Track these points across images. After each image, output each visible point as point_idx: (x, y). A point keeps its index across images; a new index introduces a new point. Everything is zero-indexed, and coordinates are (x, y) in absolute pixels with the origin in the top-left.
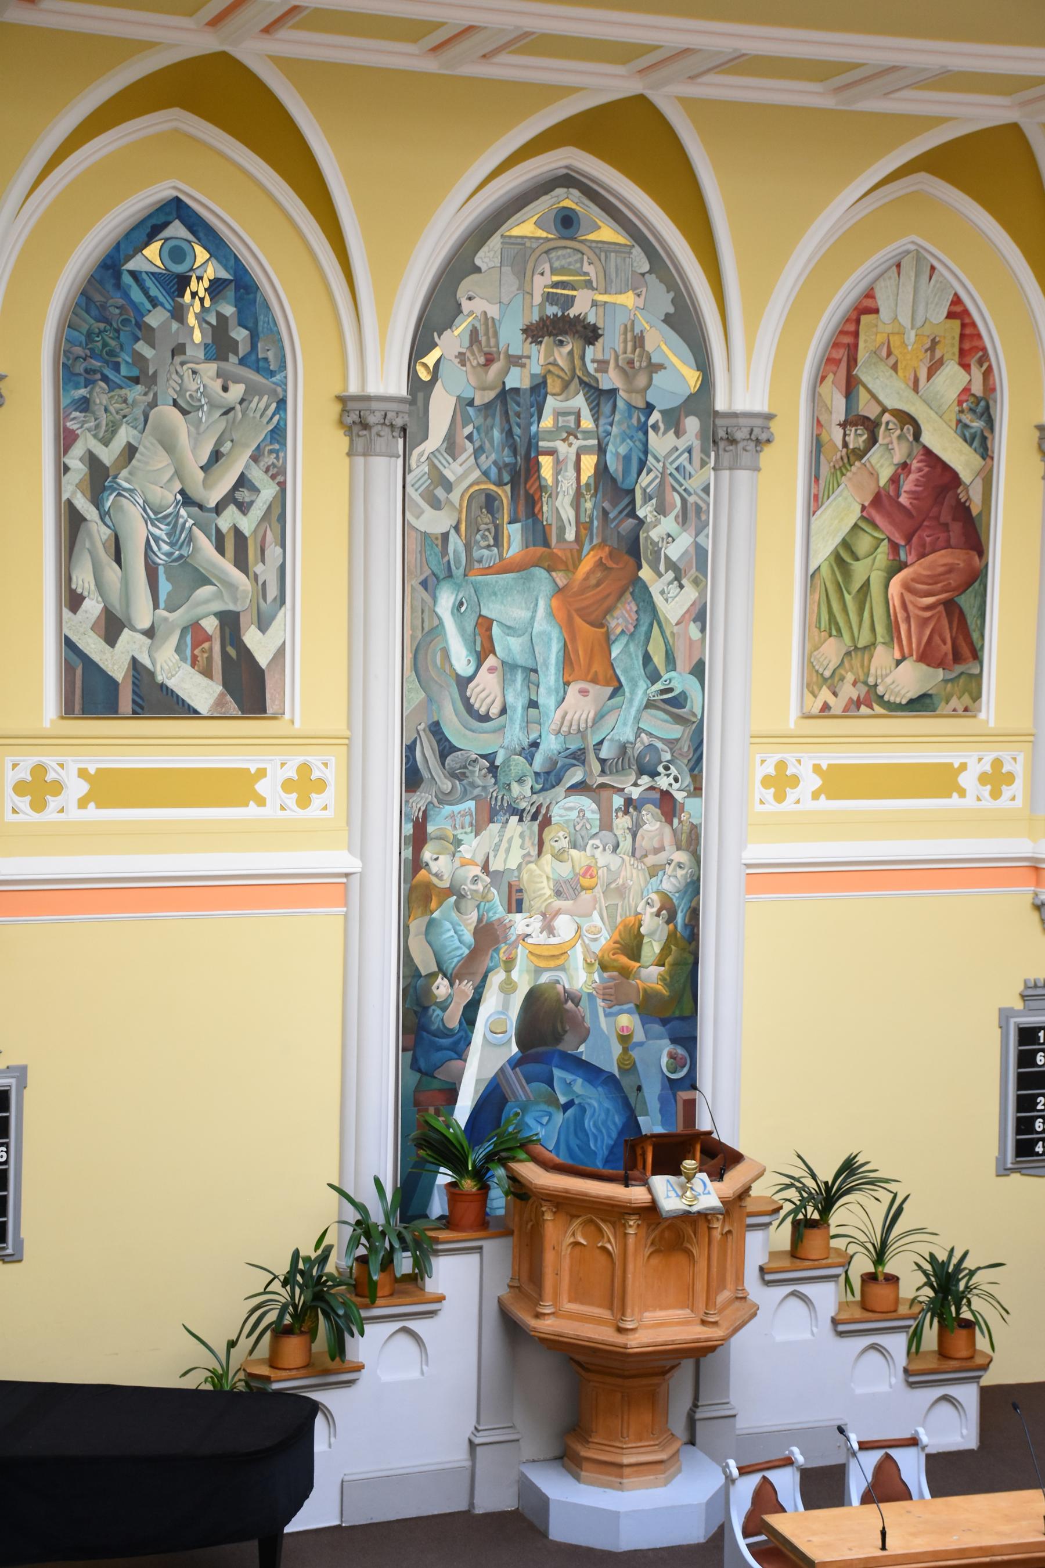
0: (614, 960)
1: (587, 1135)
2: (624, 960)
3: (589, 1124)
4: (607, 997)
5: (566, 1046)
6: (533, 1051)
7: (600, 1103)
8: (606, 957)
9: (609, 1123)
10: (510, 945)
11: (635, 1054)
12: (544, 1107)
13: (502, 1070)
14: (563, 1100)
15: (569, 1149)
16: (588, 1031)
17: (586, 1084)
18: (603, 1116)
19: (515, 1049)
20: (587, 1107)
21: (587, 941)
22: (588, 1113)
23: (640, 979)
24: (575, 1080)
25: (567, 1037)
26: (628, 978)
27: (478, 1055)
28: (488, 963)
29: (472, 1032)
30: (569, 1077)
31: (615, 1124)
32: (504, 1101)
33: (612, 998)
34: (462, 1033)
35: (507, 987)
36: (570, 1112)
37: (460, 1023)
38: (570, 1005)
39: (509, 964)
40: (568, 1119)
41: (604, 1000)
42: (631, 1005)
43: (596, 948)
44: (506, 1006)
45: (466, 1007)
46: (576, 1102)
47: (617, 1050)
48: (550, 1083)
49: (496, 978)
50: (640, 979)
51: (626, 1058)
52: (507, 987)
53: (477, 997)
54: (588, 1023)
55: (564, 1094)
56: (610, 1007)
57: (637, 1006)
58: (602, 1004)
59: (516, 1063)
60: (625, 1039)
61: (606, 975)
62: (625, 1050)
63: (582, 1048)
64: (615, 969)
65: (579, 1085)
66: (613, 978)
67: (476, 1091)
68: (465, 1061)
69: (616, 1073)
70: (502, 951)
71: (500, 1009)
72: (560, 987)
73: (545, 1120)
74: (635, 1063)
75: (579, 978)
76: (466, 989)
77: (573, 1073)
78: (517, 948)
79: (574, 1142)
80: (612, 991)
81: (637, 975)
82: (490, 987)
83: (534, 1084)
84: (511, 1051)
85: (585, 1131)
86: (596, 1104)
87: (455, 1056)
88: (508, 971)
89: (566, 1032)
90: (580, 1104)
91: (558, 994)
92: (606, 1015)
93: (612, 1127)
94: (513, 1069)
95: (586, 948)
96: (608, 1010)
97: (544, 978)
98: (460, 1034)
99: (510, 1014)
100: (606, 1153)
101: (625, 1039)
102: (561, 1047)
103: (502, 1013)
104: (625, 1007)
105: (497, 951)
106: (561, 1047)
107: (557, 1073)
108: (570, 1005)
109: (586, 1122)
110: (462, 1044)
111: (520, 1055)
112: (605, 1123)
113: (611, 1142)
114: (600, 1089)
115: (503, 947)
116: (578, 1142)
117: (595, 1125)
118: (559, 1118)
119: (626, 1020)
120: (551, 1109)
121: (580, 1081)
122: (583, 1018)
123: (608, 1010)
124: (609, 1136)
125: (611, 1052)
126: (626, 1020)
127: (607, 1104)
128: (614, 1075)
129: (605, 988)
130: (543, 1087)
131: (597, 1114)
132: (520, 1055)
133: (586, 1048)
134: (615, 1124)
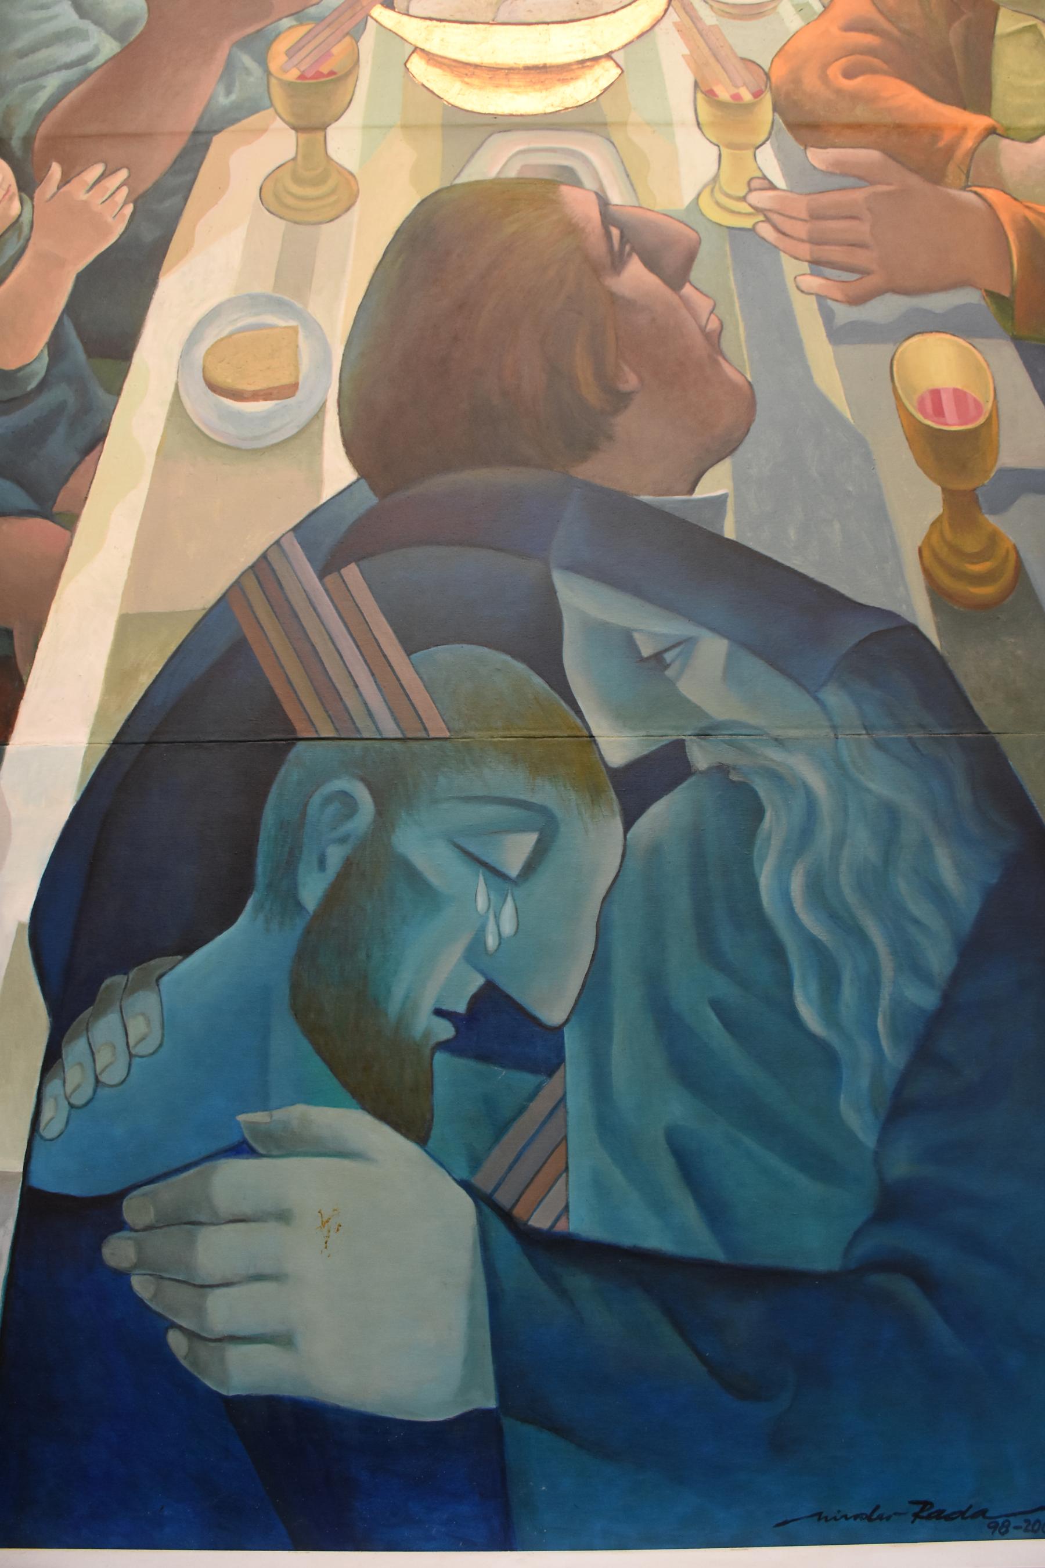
0: (855, 97)
1: (777, 951)
2: (907, 99)
3: (780, 884)
4: (835, 253)
5: (633, 462)
6: (440, 484)
7: (842, 776)
8: (811, 82)
9: (903, 886)
10: (320, 20)
11: (1015, 526)
12: (504, 778)
13: (263, 569)
14: (618, 746)
15: (664, 1017)
16: (748, 401)
17: (755, 667)
18: (862, 844)
19: (337, 472)
20: (762, 788)
21: (708, 17)
22: (776, 826)
23: (1000, 186)
24: (686, 644)
25: (627, 423)
26: (935, 176)
27: (138, 497)
28: (207, 90)
29: (116, 391)
30: (652, 627)
31: (936, 892)
32: (271, 740)
33: (861, 258)
34: (60, 393)
35: (309, 194)
36: (663, 814)
37: (56, 346)
38: (635, 277)
39: (315, 104)
40: (655, 851)
41: (817, 264)
42: (970, 297)
43: (758, 42)
44: (294, 277)
45: (79, 277)
46: (700, 757)
47: (916, 504)
48: (539, 644)
49: (251, 157)
50: (1000, 186)
51: (971, 544)
52: (309, 194)
53: (149, 234)
54: (741, 357)
55: (623, 715)
56: (857, 300)
57: (992, 295)
58: (813, 282)
59: (334, 541)
60: (953, 450)
61: (819, 157)
62: (962, 507)
63: (716, 483)
64: (858, 131)
65: (710, 673)
66: (864, 177)
67: (117, 675)
68: (69, 522)
69: (924, 617)
70: (279, 50)
71: (264, 286)
72: (580, 204)
73: (515, 851)
74: (1020, 567)
75: (684, 169)
76: (96, 199)
77: (670, 607)
78: (356, 33)
79: (693, 987)
80: (862, 230)
81: (979, 169)
82: (221, 188)
83: (443, 654)
84: (318, 482)
85: (764, 924)
86: (816, 781)
87: (24, 501)
88: (311, 126)
89: (620, 400)
90: (722, 769)
91: (572, 229)
92: (837, 334)
93: (920, 909)
94: (328, 567)
95: (708, 54)
96: (844, 314)
97: (494, 162)
98: (60, 393)
99: (316, 308)
100: (895, 1057)
101: (953, 450)
102: (601, 470)
103: (278, 305)
104: (939, 302)
105: (259, 45)
106: (601, 470)
107: (579, 600)
108: (635, 277)
109: (765, 879)
110: (57, 445)
111: (368, 499)
112: (876, 883)
113: (925, 998)
114: (834, 697)
115: (290, 34)
116: (723, 987)
117: (818, 889)
118: (600, 845)
119: (939, 362)
120: (545, 794)
121: (713, 649)
122: (714, 340)
123: (844, 314)
124: (911, 964)
125: (880, 513)
126: (939, 362)
127: (883, 781)
128: (915, 629)
129: (815, 216)
130: (506, 673)
131: (825, 833)
132: (368, 499)
133: (739, 479)
134: (936, 892)
